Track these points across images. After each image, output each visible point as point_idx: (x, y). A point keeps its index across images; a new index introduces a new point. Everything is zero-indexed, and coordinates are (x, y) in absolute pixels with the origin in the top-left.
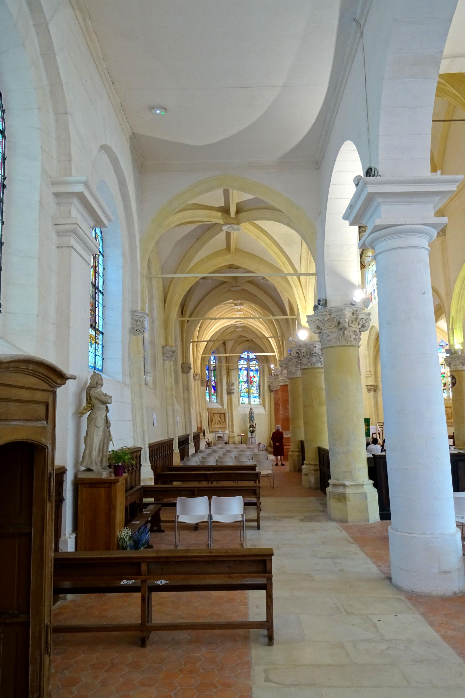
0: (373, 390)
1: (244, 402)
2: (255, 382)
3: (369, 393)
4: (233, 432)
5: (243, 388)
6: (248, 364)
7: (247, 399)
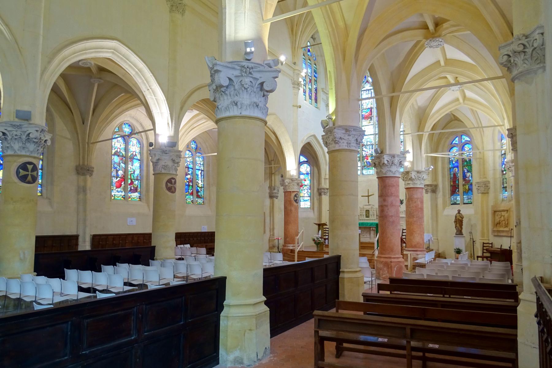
0: (430, 191)
4: (273, 235)
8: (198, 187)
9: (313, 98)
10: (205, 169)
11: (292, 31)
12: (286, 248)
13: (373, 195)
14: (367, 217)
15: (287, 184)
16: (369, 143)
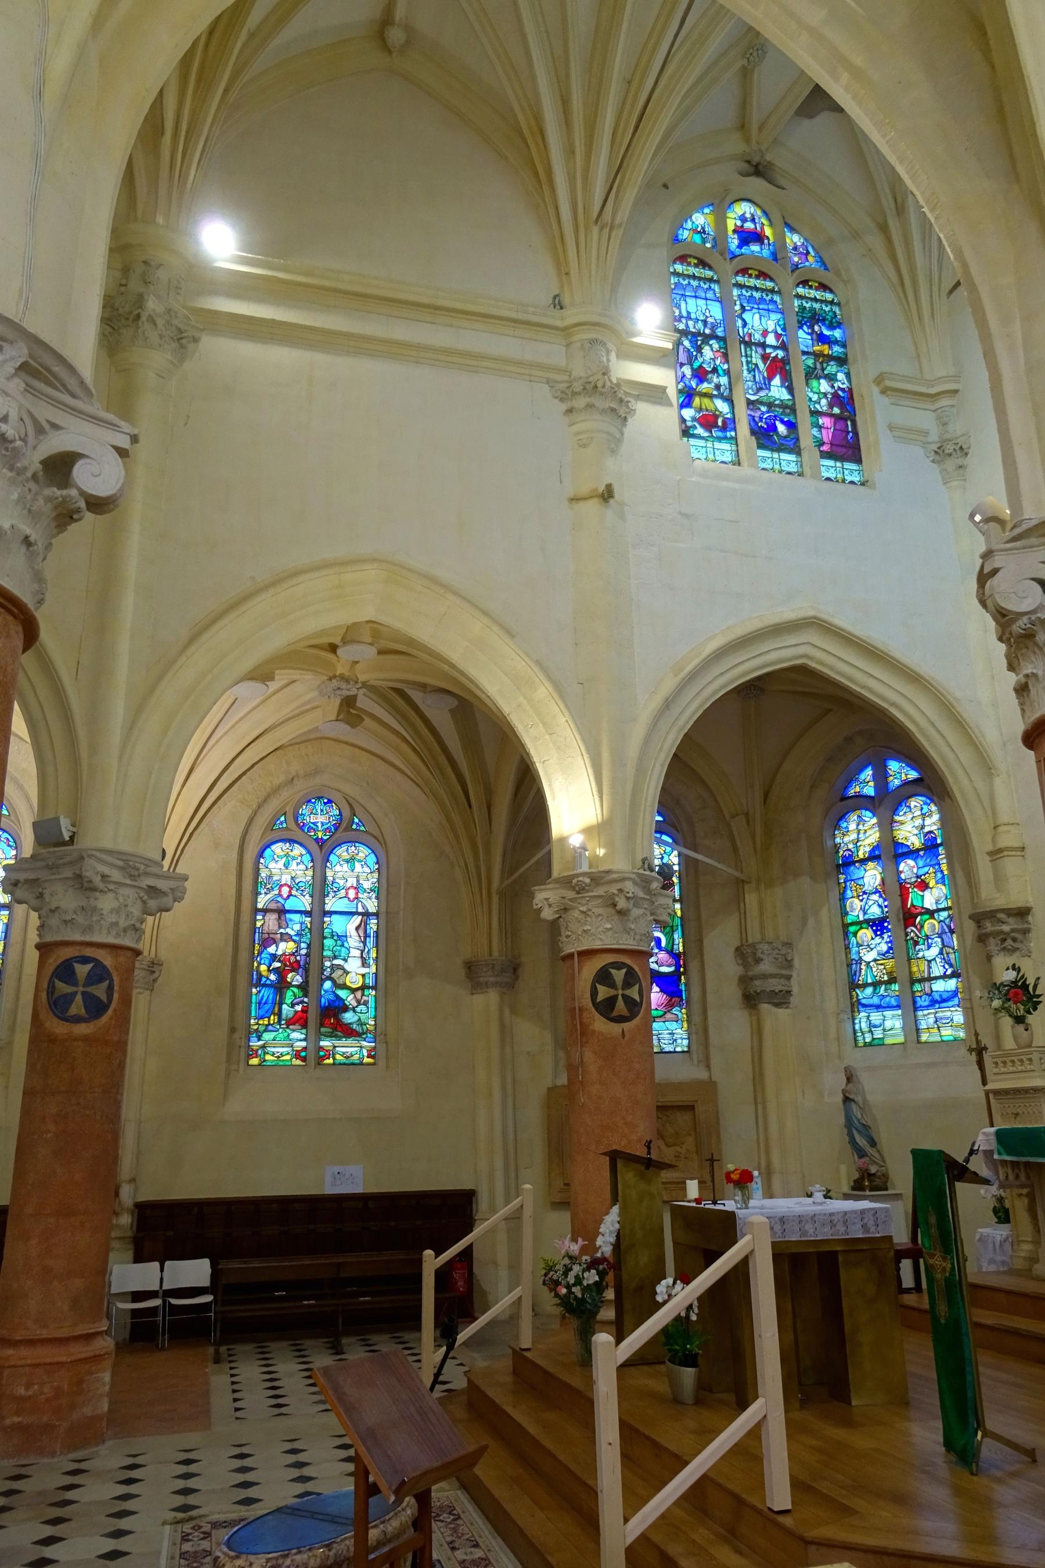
1: (878, 1034)
2: (931, 913)
5: (869, 956)
6: (887, 825)
7: (894, 1021)
8: (344, 987)
10: (383, 909)
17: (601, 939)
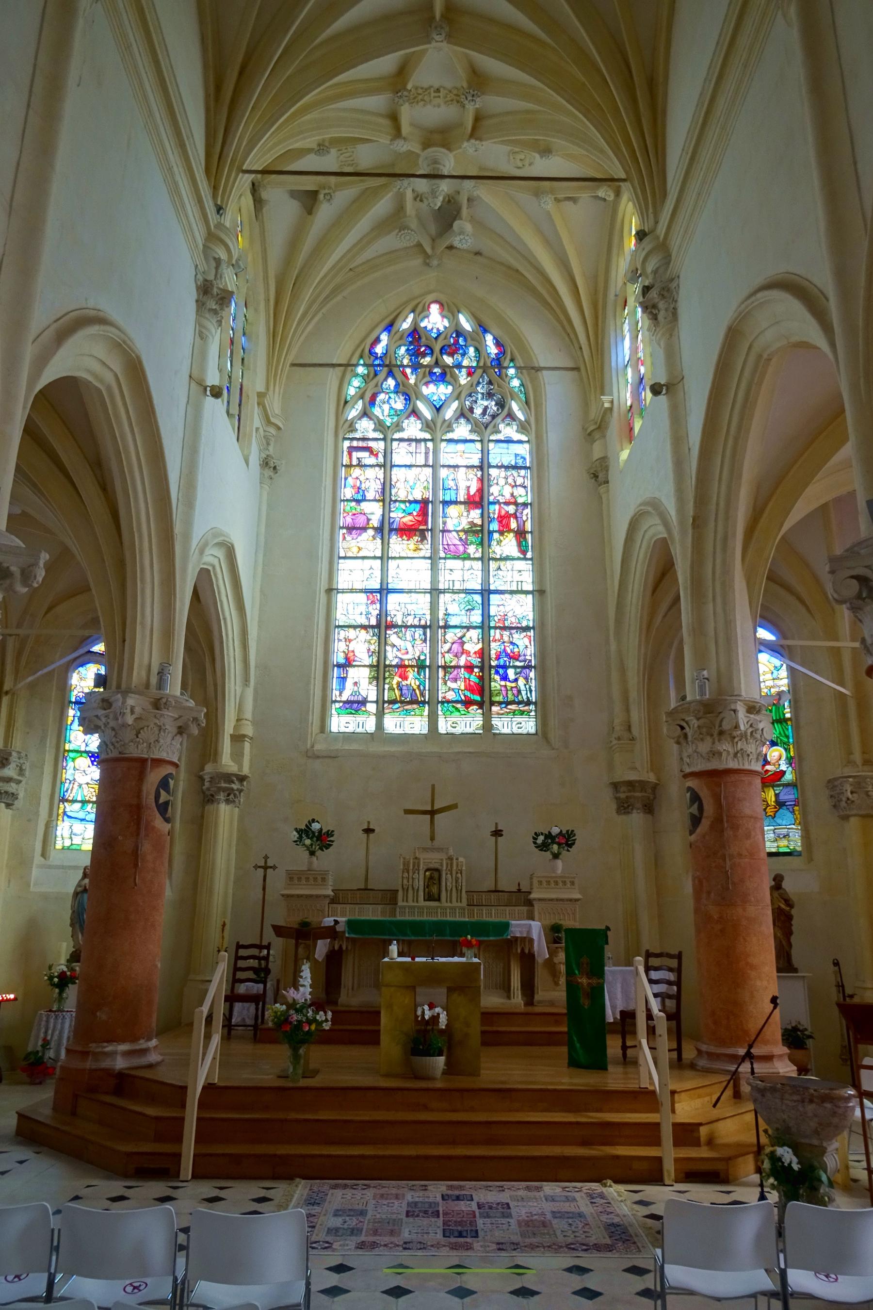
0: (639, 805)
3: (624, 817)
5: (81, 779)
9: (235, 410)
11: (218, 88)
12: (89, 1064)
13: (454, 807)
14: (429, 897)
15: (130, 719)
16: (410, 621)
17: (168, 753)
